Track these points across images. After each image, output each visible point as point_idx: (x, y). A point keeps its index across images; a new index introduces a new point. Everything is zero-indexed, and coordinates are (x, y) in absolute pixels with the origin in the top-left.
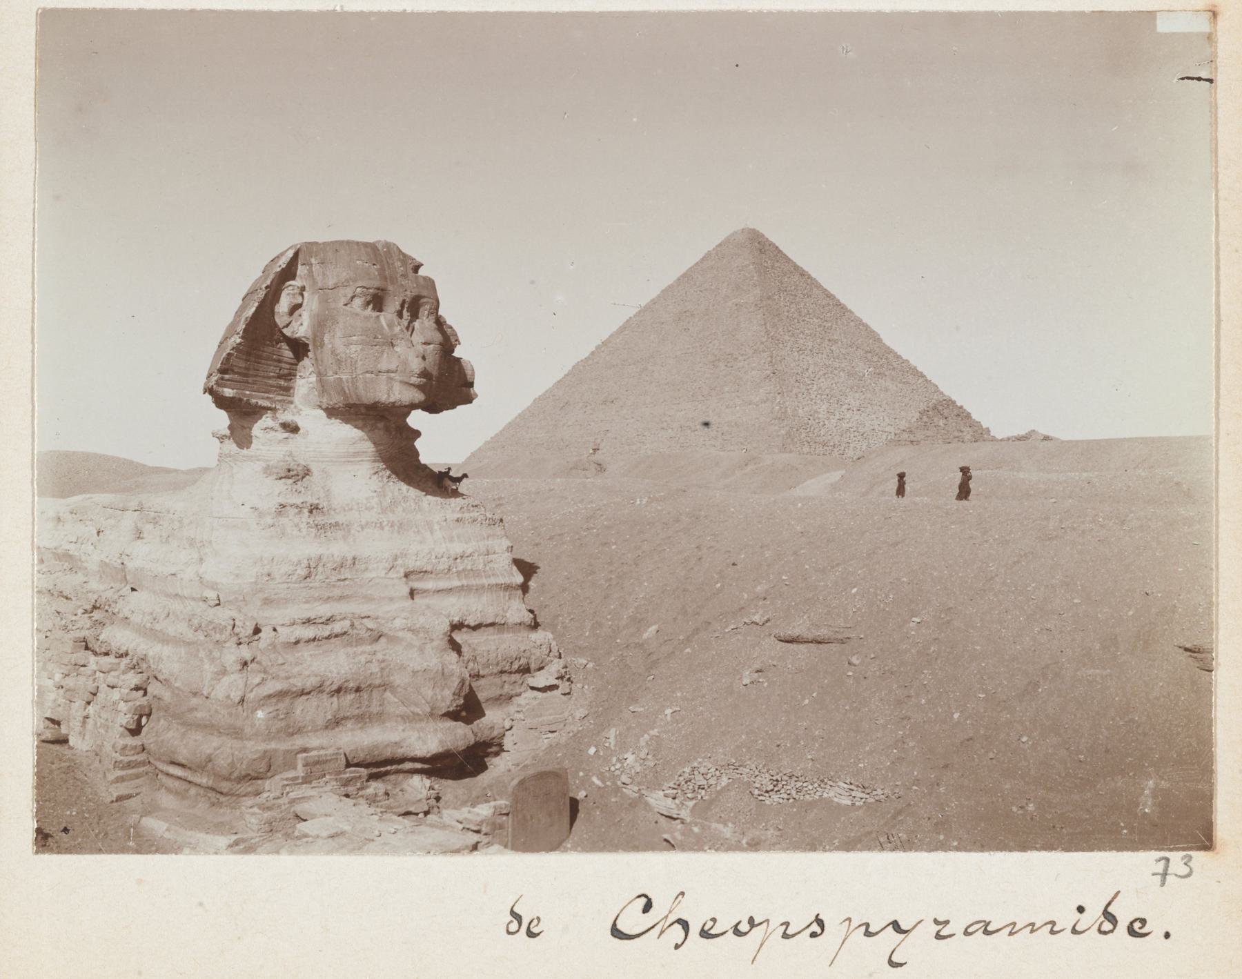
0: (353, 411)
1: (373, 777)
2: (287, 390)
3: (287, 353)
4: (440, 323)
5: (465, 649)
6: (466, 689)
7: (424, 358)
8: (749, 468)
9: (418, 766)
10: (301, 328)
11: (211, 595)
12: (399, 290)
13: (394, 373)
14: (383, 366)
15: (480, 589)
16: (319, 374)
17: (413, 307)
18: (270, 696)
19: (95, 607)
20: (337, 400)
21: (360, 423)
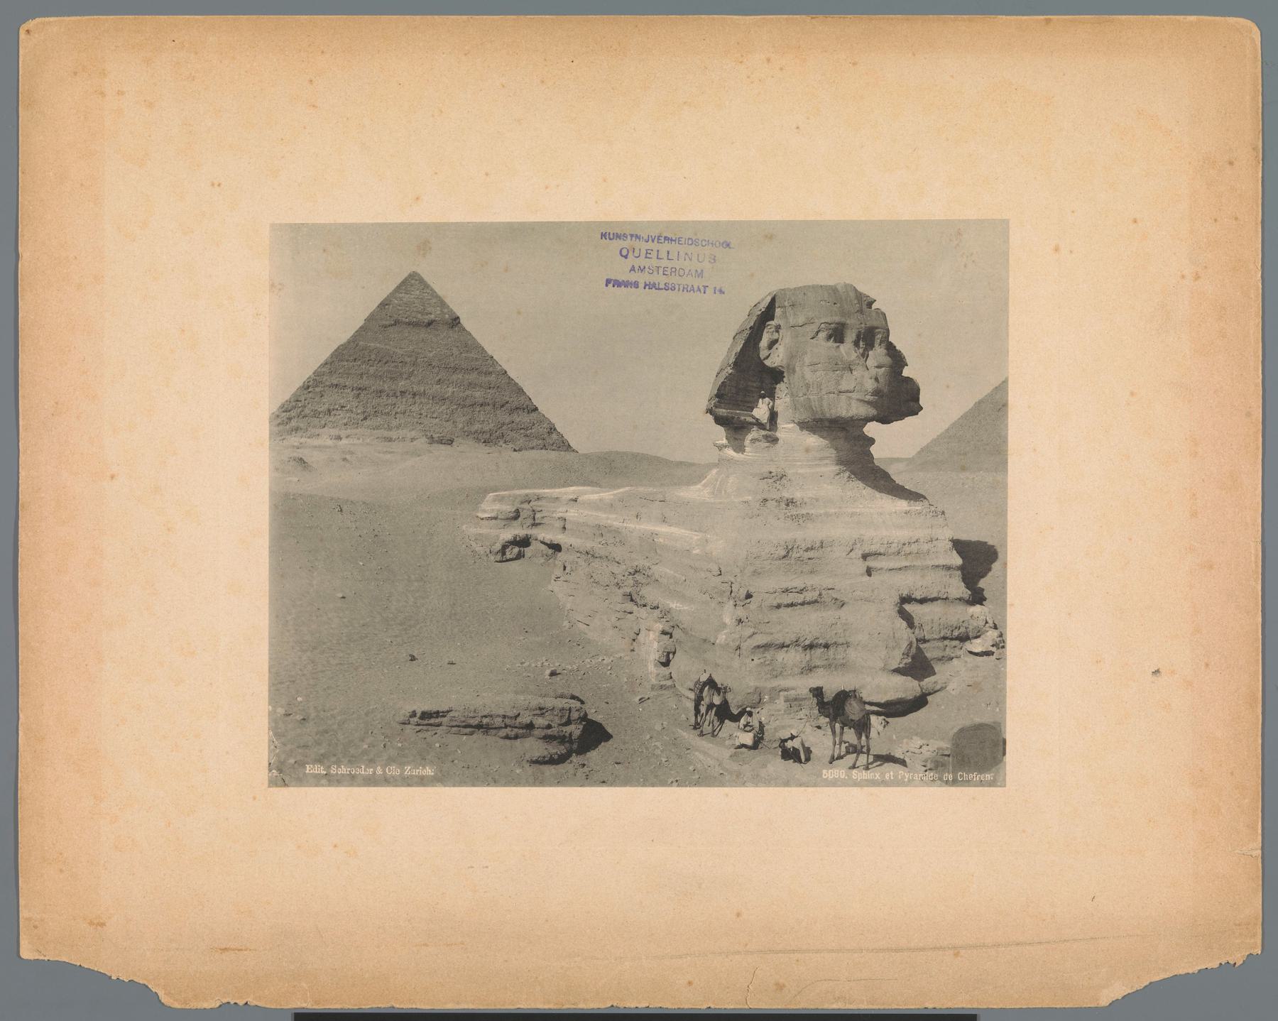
0: (819, 424)
4: (891, 349)
6: (913, 650)
7: (876, 379)
10: (776, 359)
13: (853, 389)
14: (844, 386)
18: (758, 647)
20: (805, 416)
21: (825, 434)
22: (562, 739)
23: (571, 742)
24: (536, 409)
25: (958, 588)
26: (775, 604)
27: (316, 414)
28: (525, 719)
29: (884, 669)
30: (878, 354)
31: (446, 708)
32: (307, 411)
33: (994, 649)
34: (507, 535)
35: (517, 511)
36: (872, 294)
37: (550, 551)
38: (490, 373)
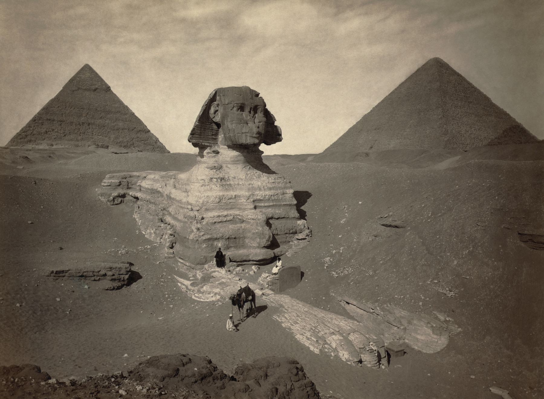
1: (238, 266)
2: (216, 139)
3: (215, 127)
5: (273, 226)
6: (271, 239)
7: (258, 127)
8: (423, 156)
9: (255, 263)
10: (218, 118)
11: (189, 207)
12: (251, 103)
13: (248, 132)
14: (244, 131)
16: (224, 134)
17: (255, 109)
18: (206, 240)
19: (164, 209)
20: (230, 143)
22: (119, 280)
23: (124, 281)
24: (149, 131)
25: (294, 213)
26: (213, 222)
27: (40, 133)
28: (103, 272)
29: (258, 247)
30: (260, 116)
31: (67, 269)
32: (35, 132)
33: (307, 237)
34: (115, 194)
35: (120, 182)
36: (258, 91)
37: (135, 200)
38: (126, 114)
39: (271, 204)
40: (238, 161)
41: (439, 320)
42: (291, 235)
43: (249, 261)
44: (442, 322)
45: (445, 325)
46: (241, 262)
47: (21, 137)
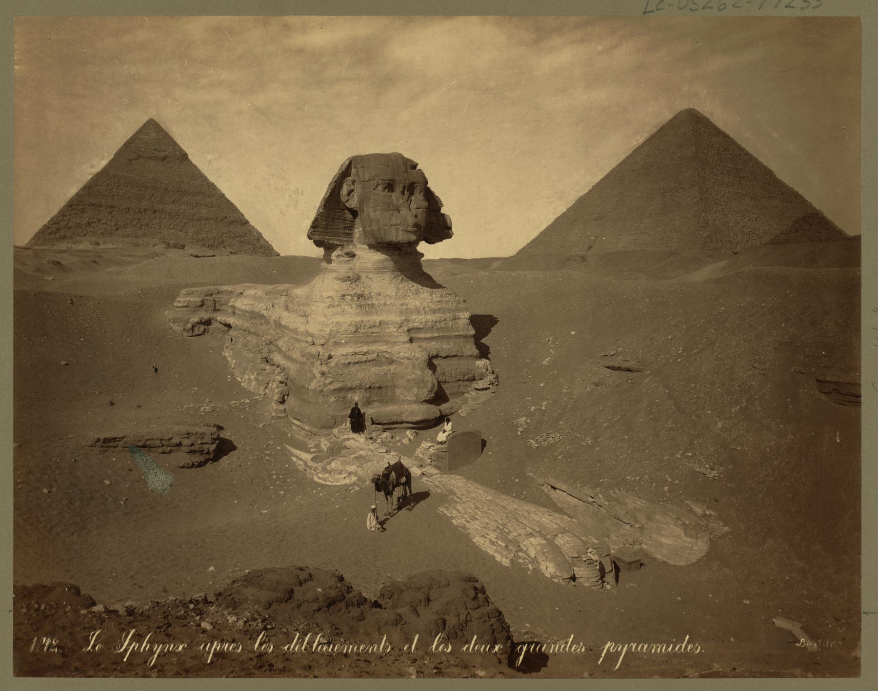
0: (380, 245)
1: (385, 430)
2: (350, 234)
3: (349, 216)
5: (438, 369)
6: (436, 389)
7: (416, 216)
8: (669, 260)
9: (411, 425)
10: (353, 203)
11: (310, 339)
12: (404, 179)
13: (401, 223)
14: (393, 222)
15: (449, 337)
16: (364, 227)
17: (410, 189)
18: (335, 390)
20: (372, 241)
22: (201, 452)
23: (208, 453)
24: (248, 222)
25: (471, 349)
26: (347, 362)
28: (176, 440)
29: (415, 402)
30: (418, 199)
31: (121, 436)
32: (71, 224)
34: (195, 319)
35: (203, 301)
36: (415, 159)
37: (226, 328)
39: (435, 335)
40: (384, 268)
41: (695, 514)
42: (465, 383)
43: (402, 423)
44: (699, 517)
45: (703, 522)
46: (389, 424)
47: (49, 231)
